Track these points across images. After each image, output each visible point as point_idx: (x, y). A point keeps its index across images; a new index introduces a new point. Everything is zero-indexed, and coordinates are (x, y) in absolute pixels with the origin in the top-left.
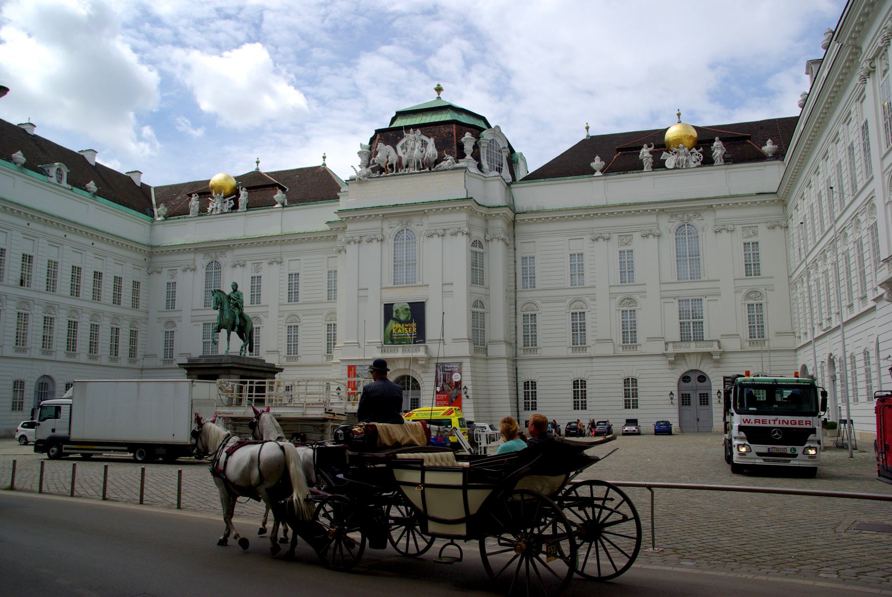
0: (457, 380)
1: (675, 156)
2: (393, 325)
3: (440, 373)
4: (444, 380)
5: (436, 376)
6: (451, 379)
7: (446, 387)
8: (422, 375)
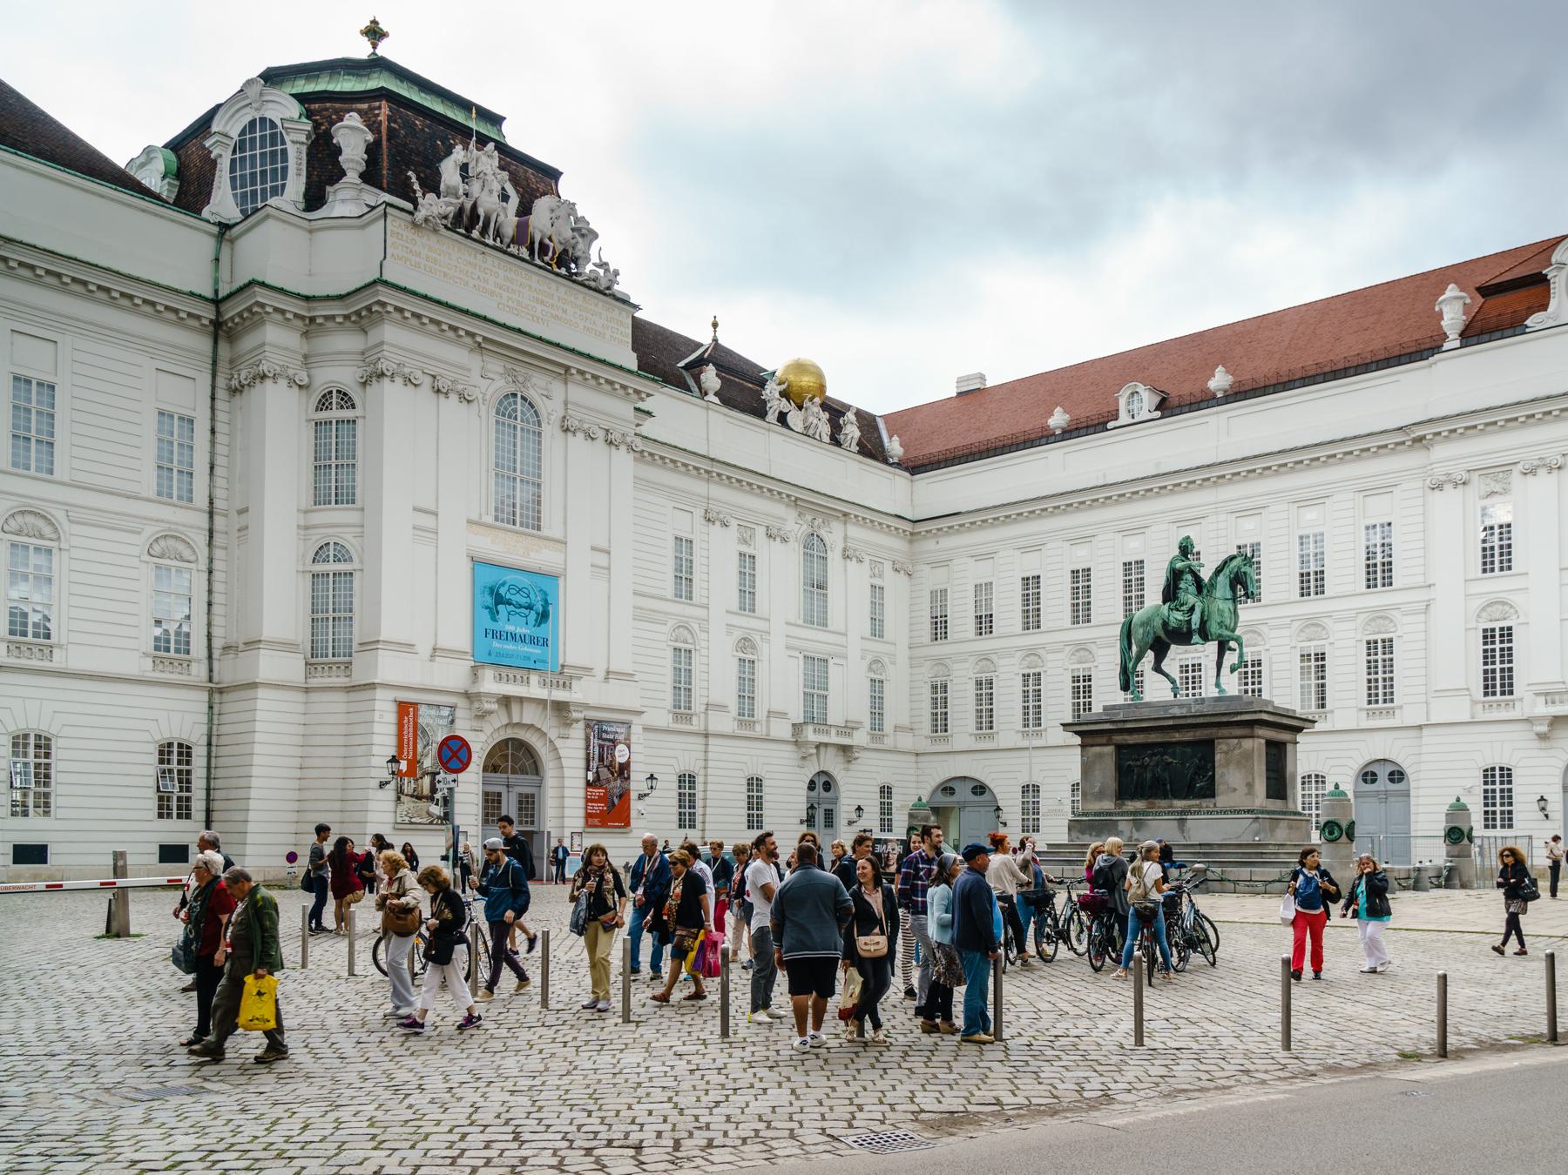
0: (623, 760)
1: (800, 414)
4: (601, 759)
6: (613, 756)
8: (559, 743)
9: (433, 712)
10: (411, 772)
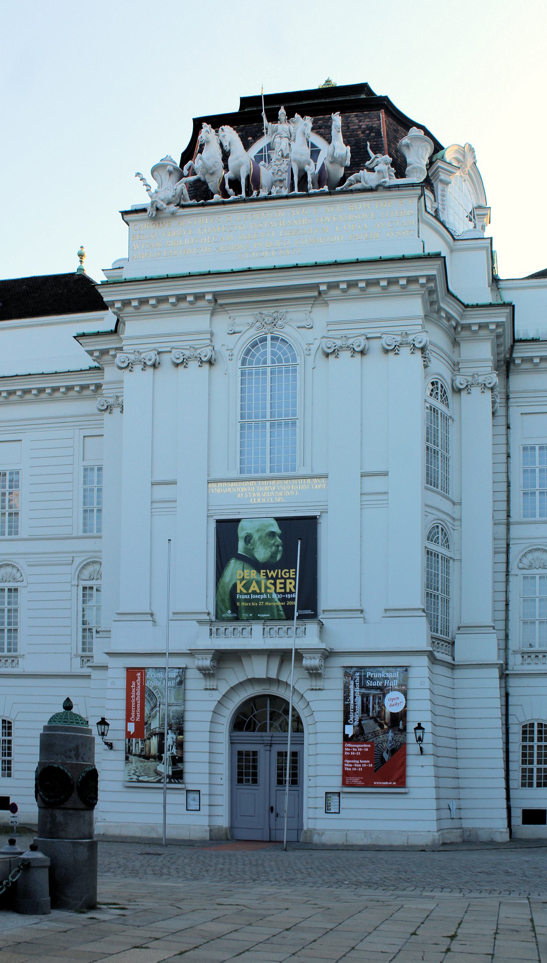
0: (397, 709)
2: (235, 571)
3: (356, 692)
4: (365, 709)
5: (346, 698)
6: (382, 706)
7: (370, 725)
8: (309, 696)
9: (160, 675)
10: (139, 733)
